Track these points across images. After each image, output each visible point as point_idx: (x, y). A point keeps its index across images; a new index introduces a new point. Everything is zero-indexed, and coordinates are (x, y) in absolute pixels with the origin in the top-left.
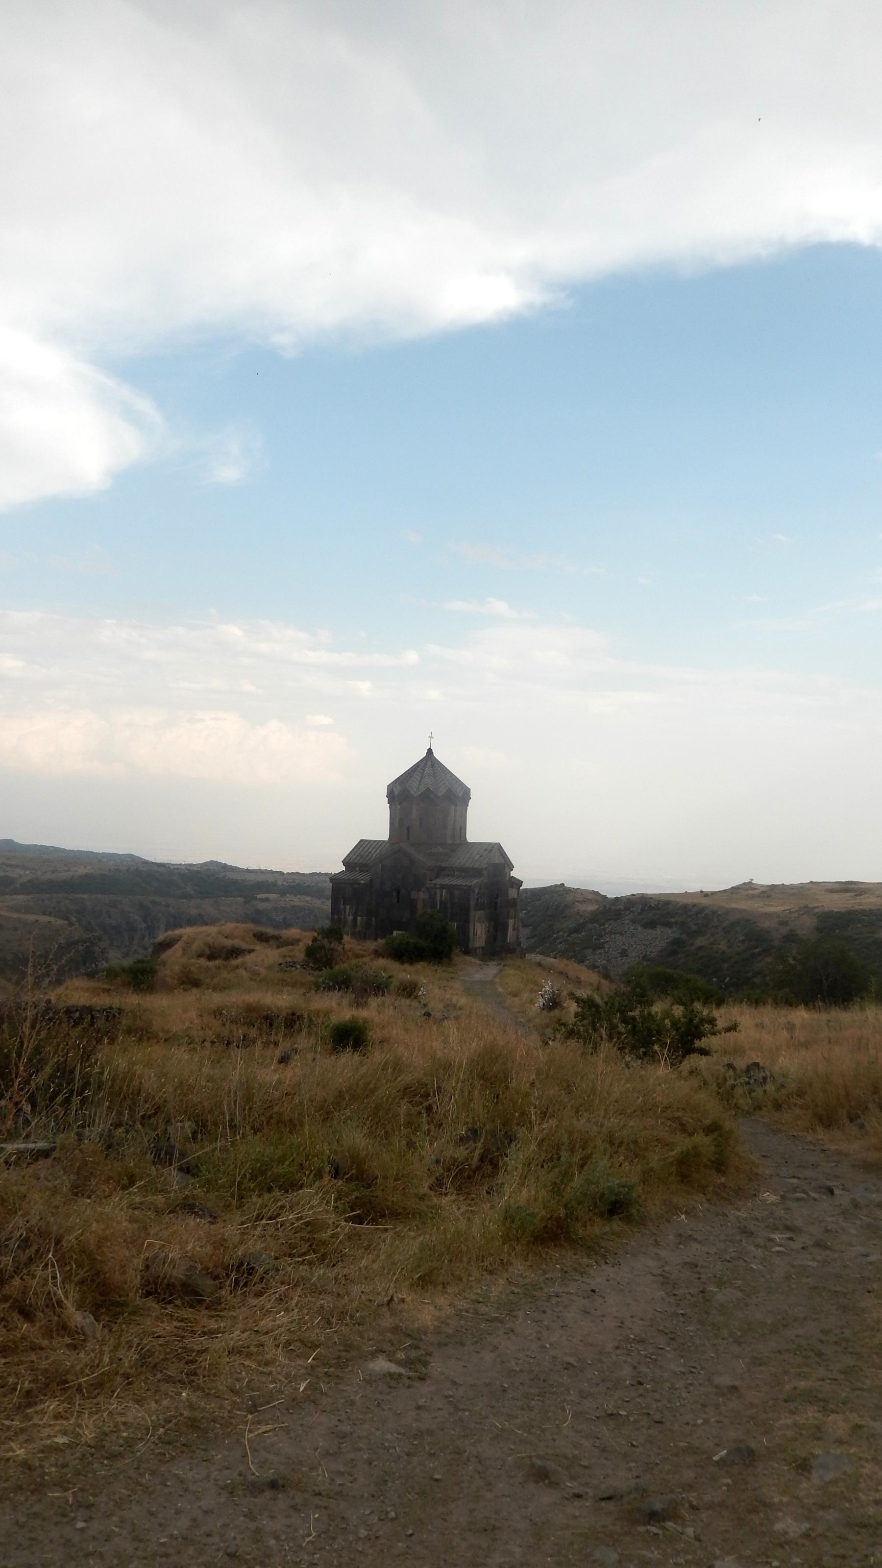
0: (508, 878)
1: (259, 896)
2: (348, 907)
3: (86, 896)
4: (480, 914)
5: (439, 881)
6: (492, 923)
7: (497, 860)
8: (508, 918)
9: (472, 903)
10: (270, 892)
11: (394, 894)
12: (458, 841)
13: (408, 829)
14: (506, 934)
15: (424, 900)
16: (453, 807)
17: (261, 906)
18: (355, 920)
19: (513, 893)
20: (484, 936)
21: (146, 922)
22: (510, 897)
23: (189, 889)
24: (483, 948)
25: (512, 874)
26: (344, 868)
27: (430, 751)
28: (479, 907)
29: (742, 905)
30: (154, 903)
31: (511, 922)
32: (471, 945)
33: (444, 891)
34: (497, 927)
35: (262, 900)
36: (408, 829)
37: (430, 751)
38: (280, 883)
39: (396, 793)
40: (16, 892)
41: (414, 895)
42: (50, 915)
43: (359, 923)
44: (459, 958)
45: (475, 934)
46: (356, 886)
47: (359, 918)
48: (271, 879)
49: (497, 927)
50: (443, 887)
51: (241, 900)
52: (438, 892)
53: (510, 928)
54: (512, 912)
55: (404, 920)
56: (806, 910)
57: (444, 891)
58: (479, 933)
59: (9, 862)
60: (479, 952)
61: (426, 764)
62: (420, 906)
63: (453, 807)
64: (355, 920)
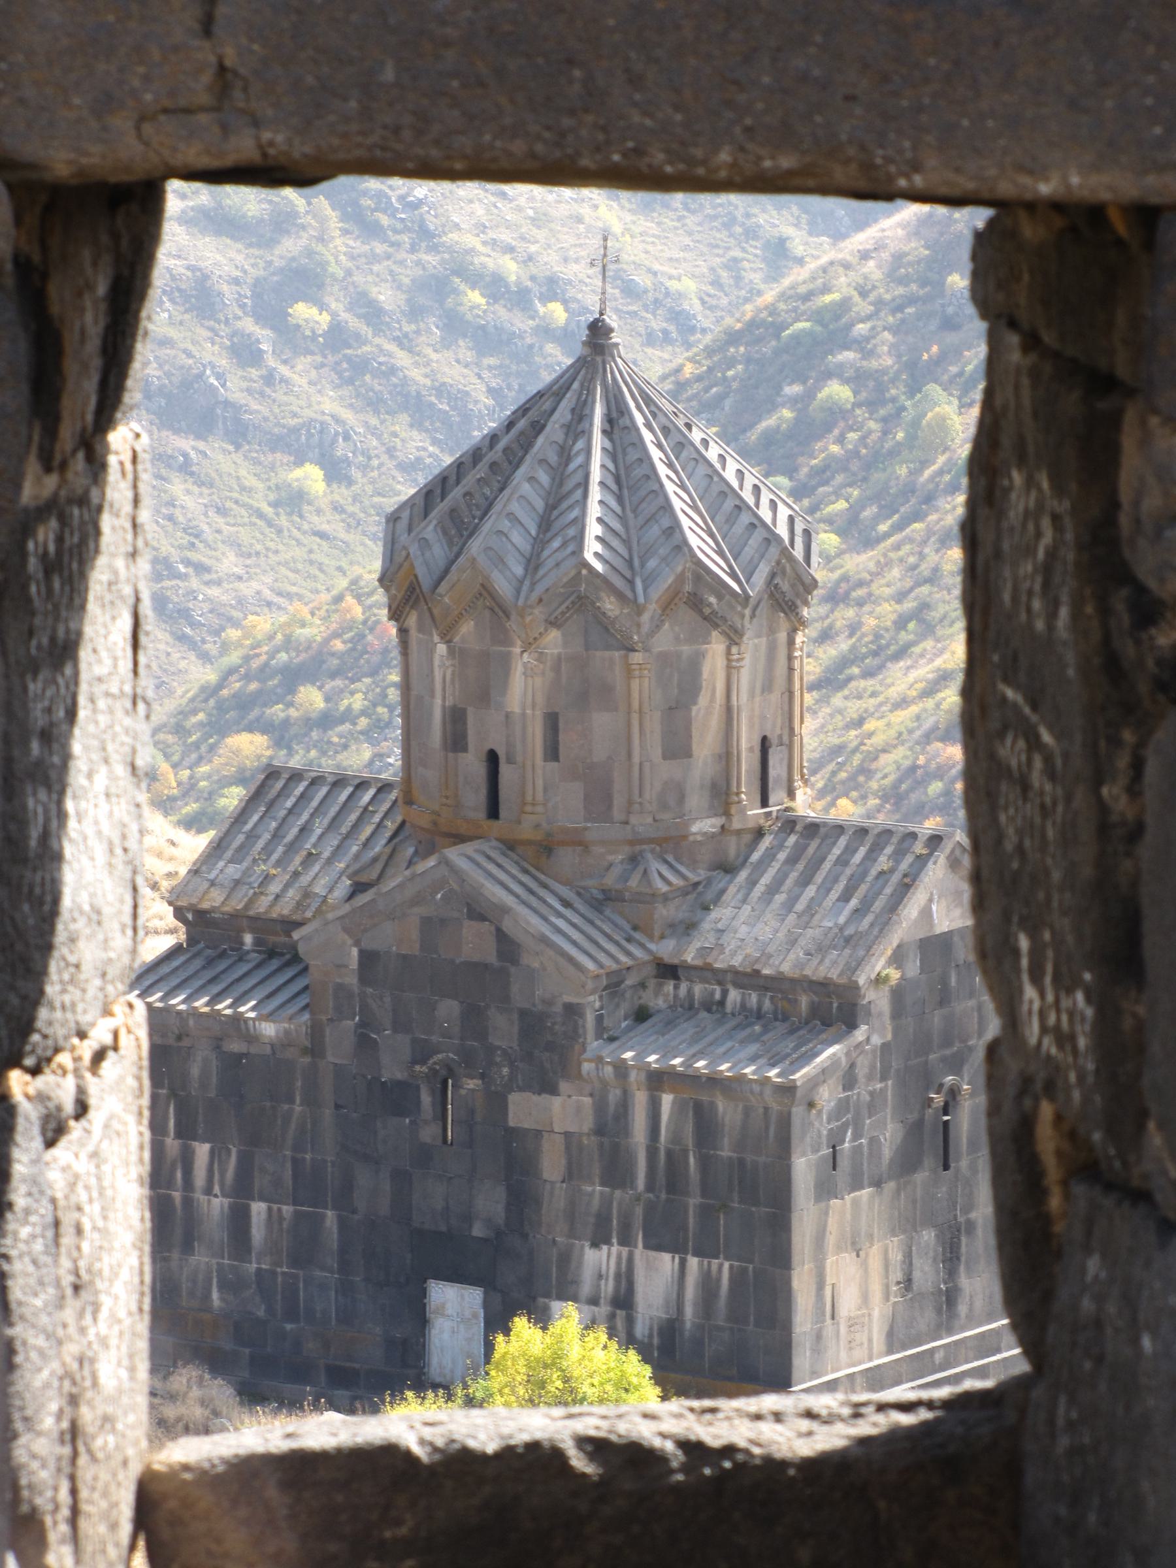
2: (202, 1151)
4: (859, 1205)
6: (928, 1236)
11: (426, 1099)
13: (493, 758)
15: (567, 1135)
16: (716, 647)
18: (239, 1219)
20: (878, 1315)
33: (667, 1100)
36: (493, 758)
41: (523, 1109)
43: (257, 1233)
45: (827, 1311)
46: (236, 1047)
47: (258, 1209)
50: (658, 1080)
52: (640, 1099)
55: (478, 1231)
57: (667, 1100)
58: (848, 1304)
61: (581, 414)
62: (552, 1165)
63: (716, 647)
64: (239, 1219)
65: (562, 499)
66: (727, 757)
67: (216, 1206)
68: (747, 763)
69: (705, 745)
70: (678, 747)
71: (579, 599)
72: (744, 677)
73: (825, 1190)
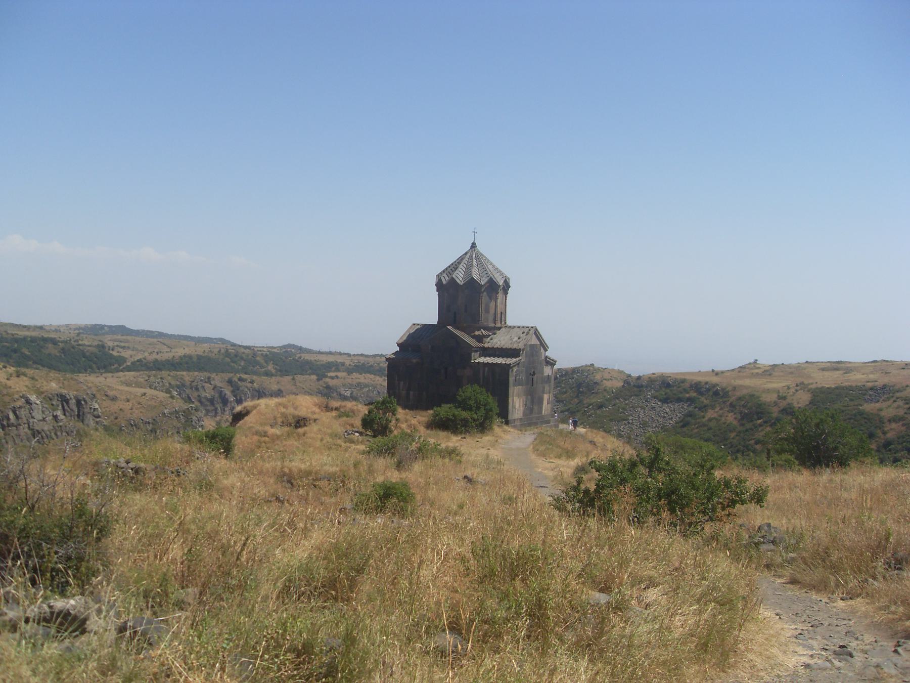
0: (543, 358)
1: (329, 374)
3: (184, 373)
5: (482, 360)
7: (534, 341)
8: (543, 392)
9: (511, 379)
10: (337, 370)
12: (498, 325)
13: (455, 313)
14: (541, 408)
17: (332, 383)
19: (547, 371)
20: (522, 409)
21: (235, 396)
22: (546, 374)
23: (270, 367)
24: (521, 419)
25: (547, 354)
26: (398, 349)
27: (474, 245)
28: (518, 383)
29: (747, 382)
30: (240, 379)
31: (546, 397)
32: (510, 418)
34: (533, 401)
35: (332, 378)
36: (455, 313)
37: (474, 245)
38: (347, 363)
39: (444, 282)
40: (128, 369)
42: (155, 388)
43: (411, 397)
44: (497, 429)
45: (514, 407)
47: (411, 393)
48: (340, 359)
49: (533, 401)
51: (314, 377)
53: (545, 402)
54: (547, 388)
56: (801, 386)
58: (517, 406)
59: (122, 344)
60: (518, 423)
65: (469, 267)
66: (495, 314)
67: (404, 393)
68: (499, 315)
69: (492, 311)
70: (487, 311)
71: (471, 283)
72: (499, 301)
73: (514, 385)
